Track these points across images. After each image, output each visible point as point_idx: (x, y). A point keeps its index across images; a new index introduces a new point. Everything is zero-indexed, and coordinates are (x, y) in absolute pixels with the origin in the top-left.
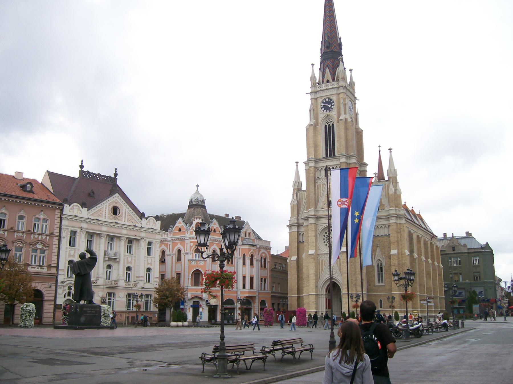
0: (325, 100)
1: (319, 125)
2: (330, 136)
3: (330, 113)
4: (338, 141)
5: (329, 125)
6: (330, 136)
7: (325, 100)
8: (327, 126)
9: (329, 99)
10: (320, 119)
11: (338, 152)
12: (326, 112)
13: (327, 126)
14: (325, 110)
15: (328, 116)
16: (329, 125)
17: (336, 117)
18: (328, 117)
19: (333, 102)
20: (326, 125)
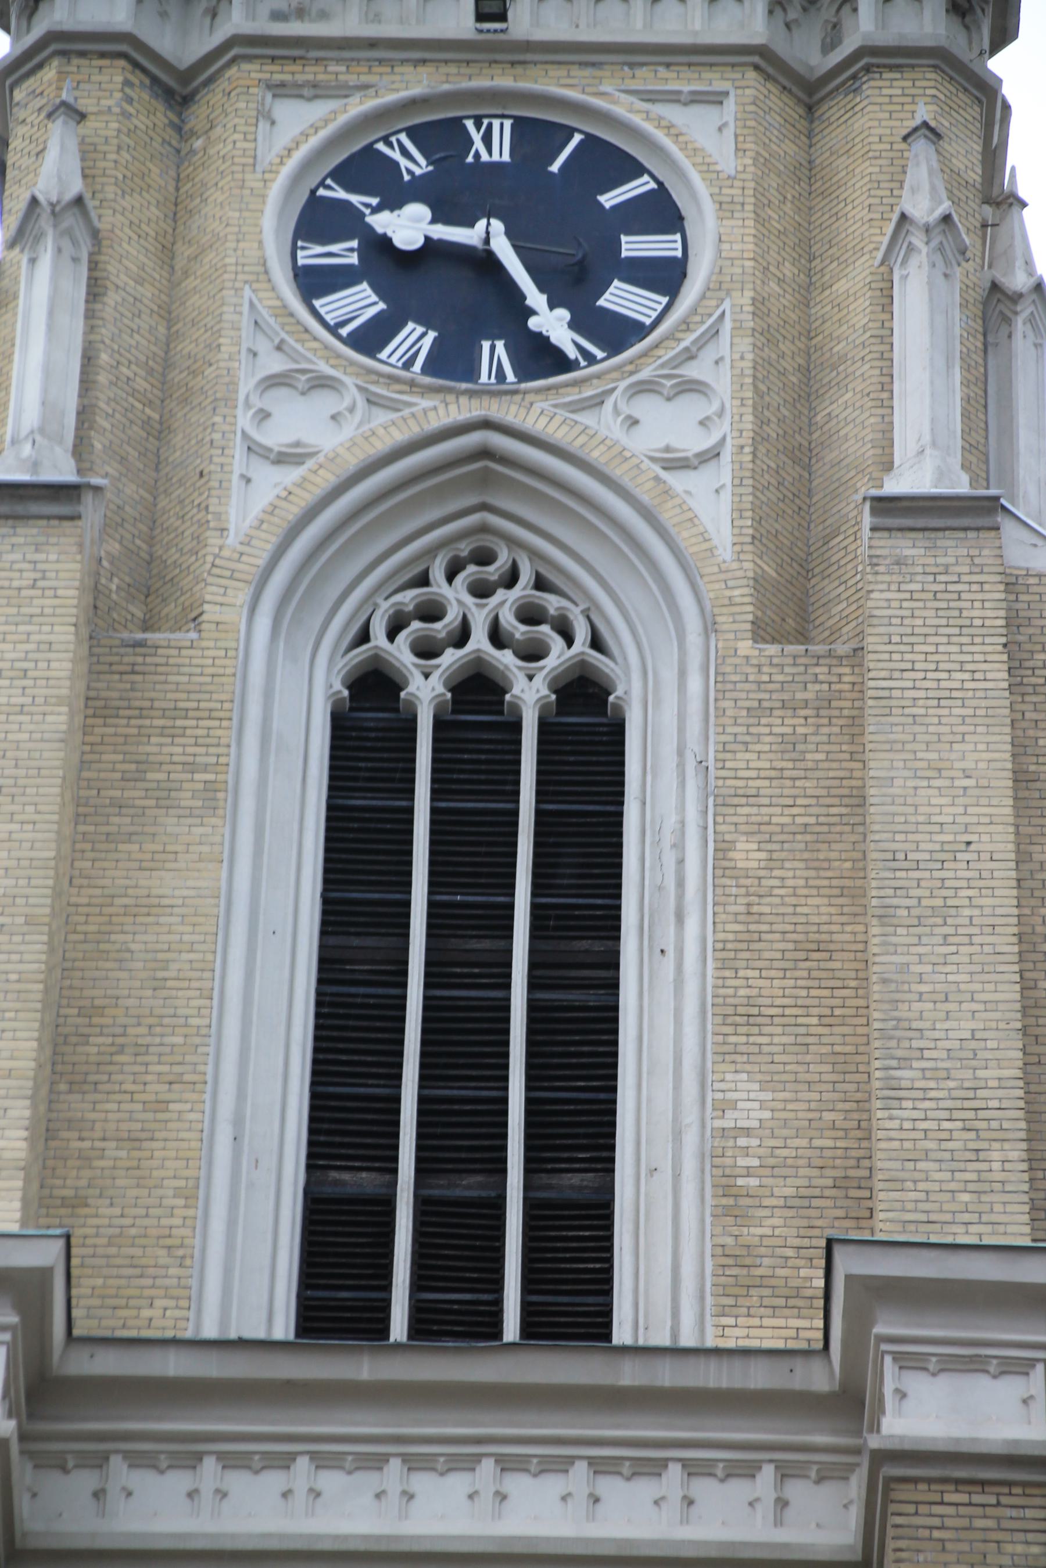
0: (441, 137)
1: (224, 603)
2: (469, 921)
3: (539, 410)
4: (736, 1022)
5: (477, 689)
6: (469, 921)
7: (441, 137)
8: (426, 691)
9: (536, 135)
10: (248, 505)
11: (738, 1277)
12: (452, 363)
13: (426, 691)
14: (415, 339)
15: (482, 466)
16: (477, 689)
17: (713, 508)
18: (471, 504)
19: (661, 212)
20: (372, 690)
